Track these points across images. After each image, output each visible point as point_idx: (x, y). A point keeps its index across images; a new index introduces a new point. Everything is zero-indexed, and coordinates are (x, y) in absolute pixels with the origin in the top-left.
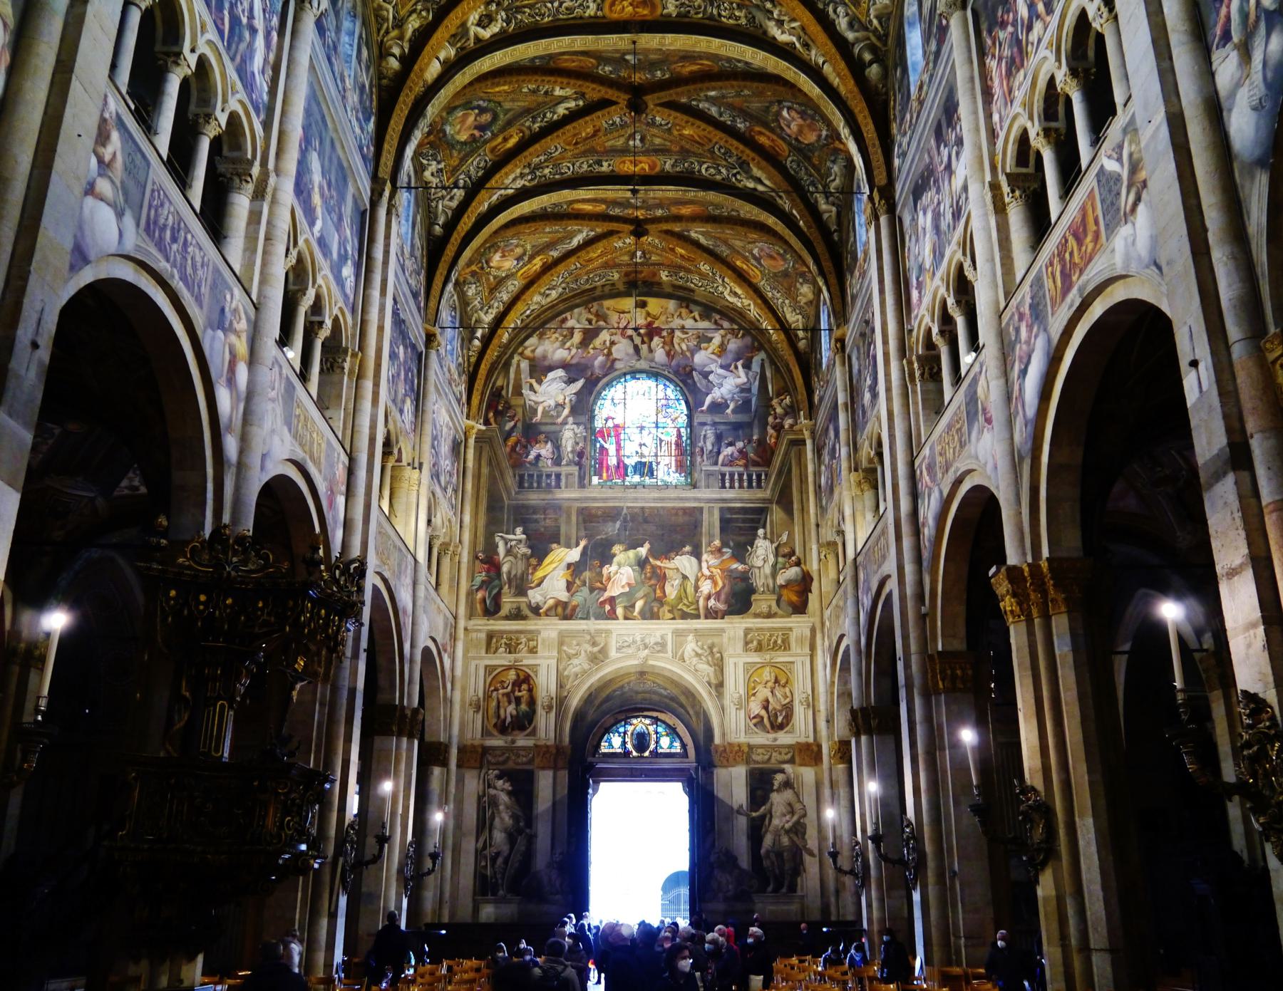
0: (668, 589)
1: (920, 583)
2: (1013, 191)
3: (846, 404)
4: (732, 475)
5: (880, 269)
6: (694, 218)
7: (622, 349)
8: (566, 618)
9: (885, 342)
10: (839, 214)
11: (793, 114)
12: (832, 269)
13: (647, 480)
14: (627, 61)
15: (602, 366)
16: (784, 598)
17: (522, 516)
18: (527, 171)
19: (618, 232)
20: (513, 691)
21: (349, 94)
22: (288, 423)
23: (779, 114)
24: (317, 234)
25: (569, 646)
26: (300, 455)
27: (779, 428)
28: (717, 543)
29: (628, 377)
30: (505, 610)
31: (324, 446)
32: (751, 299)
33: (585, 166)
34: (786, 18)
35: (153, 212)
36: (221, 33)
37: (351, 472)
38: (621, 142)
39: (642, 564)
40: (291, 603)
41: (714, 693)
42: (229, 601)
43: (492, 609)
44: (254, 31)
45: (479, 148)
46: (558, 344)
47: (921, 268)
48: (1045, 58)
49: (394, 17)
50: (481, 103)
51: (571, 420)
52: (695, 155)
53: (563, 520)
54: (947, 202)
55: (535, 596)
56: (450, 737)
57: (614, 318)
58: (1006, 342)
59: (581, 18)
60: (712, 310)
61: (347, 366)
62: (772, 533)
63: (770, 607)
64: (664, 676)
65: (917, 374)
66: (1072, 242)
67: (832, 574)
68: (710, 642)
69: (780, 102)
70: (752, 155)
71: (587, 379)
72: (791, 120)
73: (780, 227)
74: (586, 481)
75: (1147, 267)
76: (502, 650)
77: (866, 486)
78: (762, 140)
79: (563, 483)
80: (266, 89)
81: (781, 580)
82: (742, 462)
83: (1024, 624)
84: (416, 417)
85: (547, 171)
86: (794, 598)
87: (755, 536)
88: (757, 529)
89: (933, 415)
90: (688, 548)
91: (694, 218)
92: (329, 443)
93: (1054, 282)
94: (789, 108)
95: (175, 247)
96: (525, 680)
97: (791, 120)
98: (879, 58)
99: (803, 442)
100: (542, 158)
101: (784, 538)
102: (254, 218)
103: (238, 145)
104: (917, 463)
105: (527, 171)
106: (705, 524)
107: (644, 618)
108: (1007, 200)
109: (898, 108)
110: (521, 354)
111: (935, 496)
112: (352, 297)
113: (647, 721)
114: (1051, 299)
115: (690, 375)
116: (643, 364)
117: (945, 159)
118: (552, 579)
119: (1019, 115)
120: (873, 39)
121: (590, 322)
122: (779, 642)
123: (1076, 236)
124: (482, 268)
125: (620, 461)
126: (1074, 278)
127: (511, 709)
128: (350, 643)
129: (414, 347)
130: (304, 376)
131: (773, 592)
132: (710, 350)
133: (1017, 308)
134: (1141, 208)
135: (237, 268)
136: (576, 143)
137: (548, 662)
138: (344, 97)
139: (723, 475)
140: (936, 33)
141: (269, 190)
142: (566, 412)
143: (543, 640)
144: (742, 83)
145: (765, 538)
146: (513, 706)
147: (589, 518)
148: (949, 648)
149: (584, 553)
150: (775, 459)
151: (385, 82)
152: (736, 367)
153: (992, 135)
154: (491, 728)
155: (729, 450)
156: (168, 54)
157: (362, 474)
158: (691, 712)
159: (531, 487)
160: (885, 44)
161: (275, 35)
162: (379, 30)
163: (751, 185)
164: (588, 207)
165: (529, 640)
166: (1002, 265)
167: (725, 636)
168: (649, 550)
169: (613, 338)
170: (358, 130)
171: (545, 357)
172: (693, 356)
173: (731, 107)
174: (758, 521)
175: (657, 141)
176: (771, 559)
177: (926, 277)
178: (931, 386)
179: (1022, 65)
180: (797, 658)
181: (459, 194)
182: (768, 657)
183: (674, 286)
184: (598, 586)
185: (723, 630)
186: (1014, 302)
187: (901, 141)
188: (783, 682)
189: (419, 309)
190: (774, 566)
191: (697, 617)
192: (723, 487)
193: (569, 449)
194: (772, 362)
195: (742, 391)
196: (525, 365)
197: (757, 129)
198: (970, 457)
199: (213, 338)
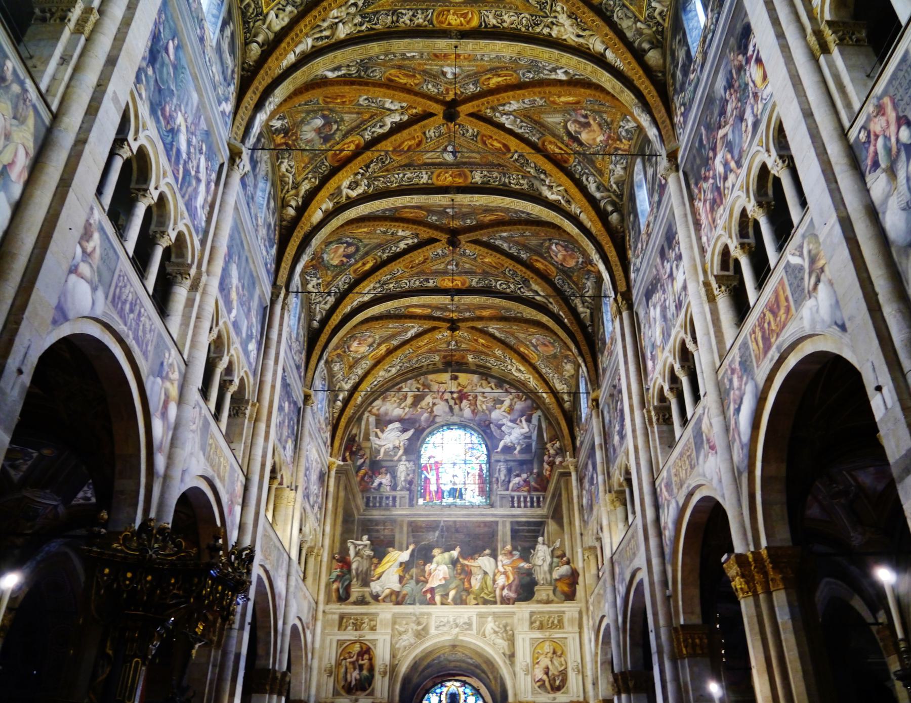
0: (473, 582)
1: (664, 572)
2: (720, 287)
3: (601, 445)
4: (519, 498)
5: (624, 347)
6: (491, 319)
7: (441, 408)
8: (398, 603)
9: (630, 398)
10: (591, 314)
11: (559, 247)
12: (588, 351)
13: (458, 502)
14: (447, 213)
15: (427, 420)
16: (559, 589)
17: (368, 527)
18: (378, 285)
19: (439, 328)
20: (357, 660)
21: (260, 228)
22: (203, 448)
23: (549, 248)
24: (232, 319)
25: (400, 625)
26: (210, 473)
27: (552, 464)
28: (509, 547)
29: (445, 428)
30: (353, 598)
31: (228, 468)
32: (531, 374)
33: (417, 283)
35: (118, 290)
36: (176, 179)
37: (246, 488)
38: (443, 266)
39: (454, 563)
40: (196, 580)
41: (508, 662)
42: (149, 578)
43: (343, 597)
44: (199, 180)
45: (345, 269)
46: (395, 405)
47: (654, 346)
48: (738, 197)
51: (404, 458)
52: (493, 275)
53: (397, 530)
54: (671, 299)
55: (375, 587)
56: (309, 696)
57: (435, 387)
58: (722, 390)
60: (503, 381)
61: (248, 412)
62: (549, 540)
63: (548, 595)
64: (470, 649)
65: (654, 419)
66: (769, 316)
67: (593, 571)
68: (504, 622)
69: (550, 240)
70: (532, 275)
71: (416, 430)
72: (558, 252)
73: (551, 323)
74: (414, 502)
75: (830, 327)
76: (350, 628)
77: (617, 504)
78: (538, 265)
79: (398, 503)
80: (204, 219)
81: (556, 575)
82: (526, 488)
83: (751, 599)
84: (295, 453)
85: (391, 286)
86: (566, 589)
87: (536, 542)
88: (537, 537)
89: (667, 449)
90: (487, 551)
91: (491, 319)
92: (232, 466)
93: (757, 344)
94: (556, 244)
95: (131, 316)
96: (366, 651)
97: (558, 252)
98: (617, 209)
99: (569, 474)
100: (389, 277)
101: (558, 544)
102: (190, 303)
103: (182, 254)
104: (657, 483)
105: (378, 285)
106: (500, 533)
107: (456, 604)
108: (716, 293)
109: (632, 240)
110: (370, 412)
111: (673, 505)
112: (254, 364)
113: (458, 684)
114: (756, 356)
115: (488, 426)
116: (455, 419)
117: (668, 270)
118: (389, 574)
119: (722, 234)
120: (614, 197)
121: (418, 389)
122: (556, 622)
123: (772, 311)
124: (345, 352)
125: (438, 488)
126: (773, 340)
127: (356, 674)
128: (238, 617)
129: (295, 403)
130: (217, 416)
131: (550, 584)
132: (503, 409)
133: (730, 365)
134: (821, 286)
135: (175, 336)
137: (385, 637)
138: (256, 230)
139: (513, 498)
140: (658, 189)
141: (202, 285)
142: (401, 452)
143: (381, 621)
144: (525, 227)
145: (544, 544)
146: (357, 672)
147: (416, 529)
148: (689, 622)
149: (412, 555)
150: (549, 486)
151: (284, 223)
152: (521, 421)
153: (703, 250)
154: (339, 688)
155: (516, 480)
156: (139, 190)
157: (254, 490)
158: (491, 677)
159: (374, 506)
160: (621, 200)
161: (213, 185)
162: (282, 190)
163: (530, 294)
164: (419, 311)
165: (371, 620)
166: (716, 337)
167: (516, 617)
168: (460, 553)
169: (435, 401)
170: (264, 253)
171: (386, 414)
172: (490, 412)
173: (517, 243)
174: (538, 531)
175: (467, 266)
176: (549, 559)
177: (658, 352)
178: (665, 428)
179: (722, 203)
180: (569, 634)
181: (331, 300)
182: (547, 634)
183: (478, 366)
184: (422, 580)
185: (514, 613)
186: (726, 362)
187: (635, 261)
188: (559, 653)
189: (300, 377)
190: (551, 564)
191: (495, 603)
192: (513, 506)
193: (403, 479)
194: (546, 418)
195: (526, 437)
196: (372, 419)
198: (699, 475)
199: (154, 383)
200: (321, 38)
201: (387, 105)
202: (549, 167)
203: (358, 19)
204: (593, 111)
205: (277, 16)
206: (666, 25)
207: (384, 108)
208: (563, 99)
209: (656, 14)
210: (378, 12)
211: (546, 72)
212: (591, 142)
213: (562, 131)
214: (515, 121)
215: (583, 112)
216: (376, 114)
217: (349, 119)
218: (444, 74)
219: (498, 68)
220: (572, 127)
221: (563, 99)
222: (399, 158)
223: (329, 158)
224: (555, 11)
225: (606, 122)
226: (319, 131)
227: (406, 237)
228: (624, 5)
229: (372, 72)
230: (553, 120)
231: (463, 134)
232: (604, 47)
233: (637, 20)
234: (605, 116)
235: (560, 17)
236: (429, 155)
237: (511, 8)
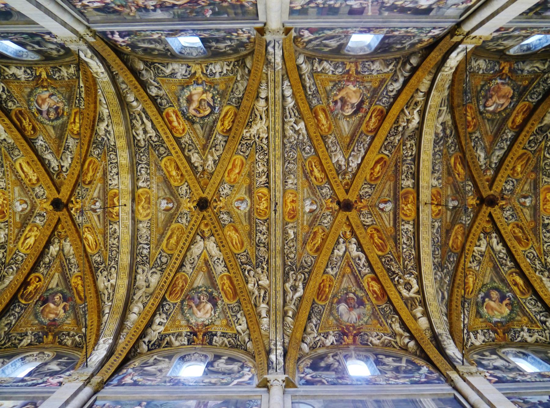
11: (490, 103)
34: (405, 118)
38: (525, 210)
45: (519, 302)
49: (390, 336)
50: (480, 296)
59: (414, 233)
69: (481, 113)
78: (519, 120)
98: (407, 61)
100: (537, 262)
120: (399, 65)
136: (527, 239)
151: (418, 353)
160: (400, 58)
162: (394, 347)
173: (492, 143)
175: (527, 187)
197: (510, 124)
200: (264, 297)
201: (341, 253)
202: (387, 125)
203: (259, 270)
204: (328, 98)
205: (240, 325)
206: (233, 60)
207: (343, 256)
208: (324, 121)
209: (229, 68)
210: (256, 256)
212: (358, 94)
213: (355, 119)
214: (354, 156)
215: (332, 105)
216: (348, 263)
217: (347, 283)
218: (312, 211)
219: (304, 172)
220: (349, 111)
221: (324, 121)
222: (389, 247)
223: (379, 303)
224: (250, 136)
225: (334, 86)
226: (351, 308)
227: (489, 244)
228: (232, 91)
229: (306, 263)
230: (346, 127)
231: (370, 195)
232: (261, 100)
233: (237, 81)
235: (253, 133)
236: (387, 223)
237: (253, 167)
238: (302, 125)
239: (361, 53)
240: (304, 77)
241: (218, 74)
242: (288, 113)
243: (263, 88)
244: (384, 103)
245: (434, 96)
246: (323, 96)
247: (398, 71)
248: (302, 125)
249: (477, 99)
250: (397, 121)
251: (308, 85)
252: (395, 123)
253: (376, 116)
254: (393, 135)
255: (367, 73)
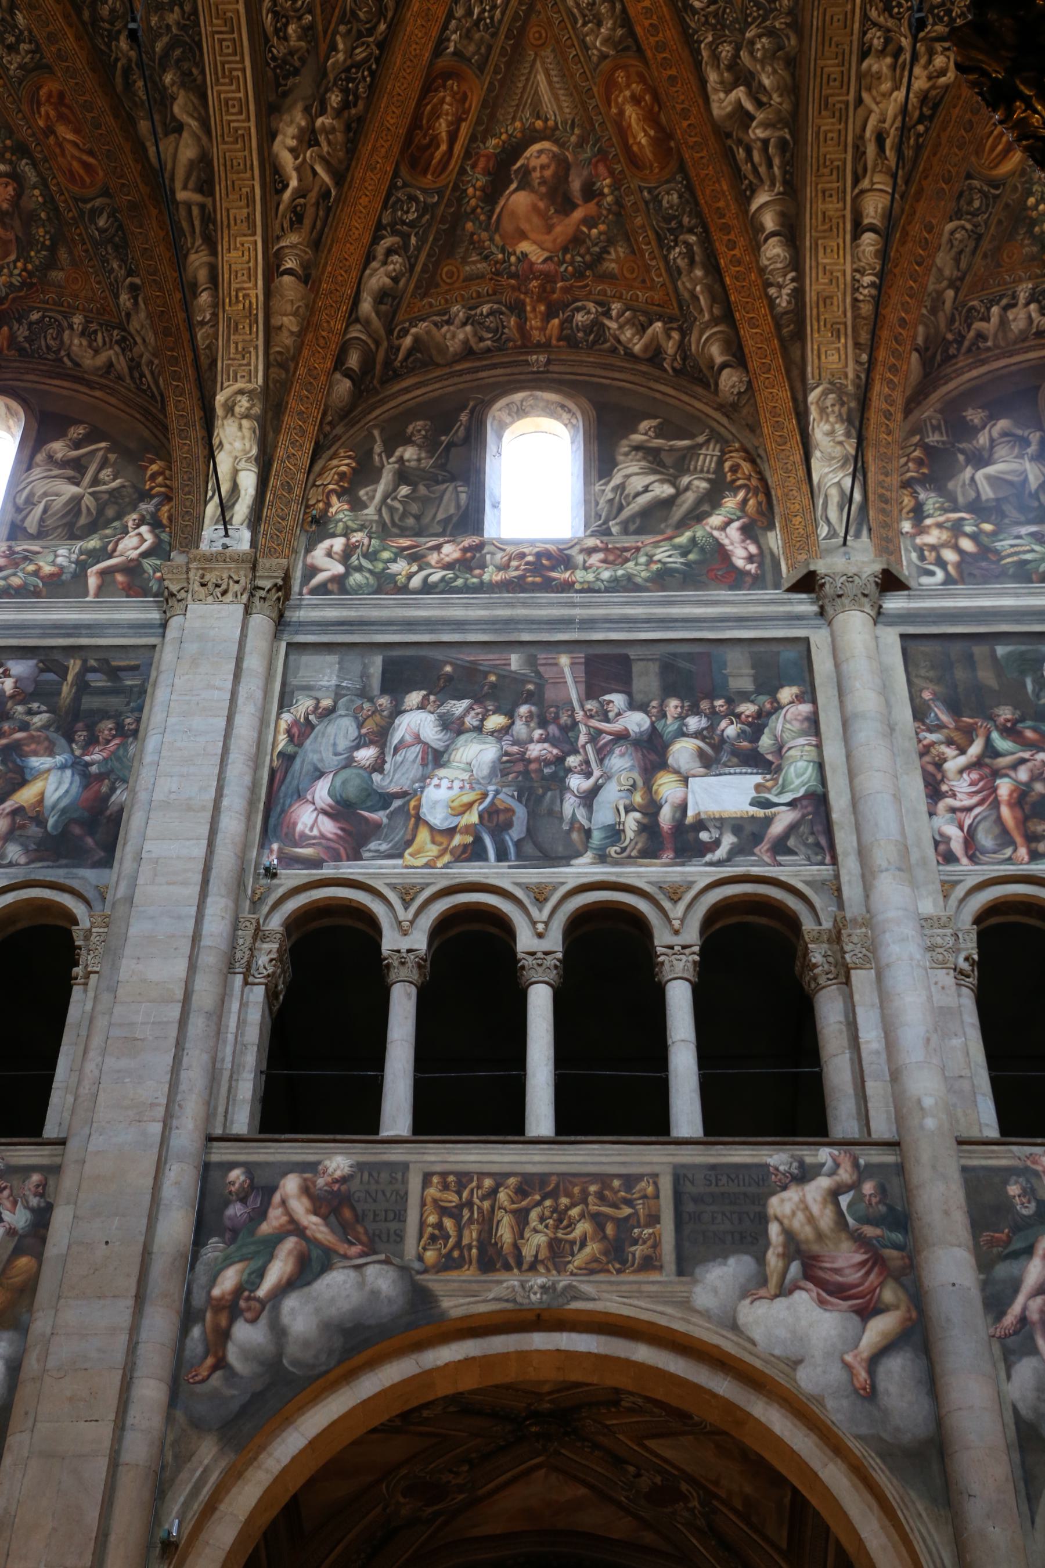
69: (22, 150)
120: (380, 357)
160: (384, 382)
202: (391, 118)
206: (961, 358)
208: (632, 114)
211: (726, 51)
212: (507, 225)
220: (538, 155)
221: (632, 114)
224: (931, 53)
225: (599, 258)
228: (979, 238)
230: (546, 90)
234: (619, 251)
238: (723, 103)
239: (518, 396)
240: (716, 311)
241: (1022, 301)
242: (776, 161)
243: (867, 280)
244: (412, 198)
245: (251, 275)
246: (639, 221)
247: (382, 332)
248: (723, 103)
249: (56, 209)
250: (355, 131)
251: (699, 273)
252: (360, 120)
253: (435, 142)
254: (358, 65)
255: (485, 309)
